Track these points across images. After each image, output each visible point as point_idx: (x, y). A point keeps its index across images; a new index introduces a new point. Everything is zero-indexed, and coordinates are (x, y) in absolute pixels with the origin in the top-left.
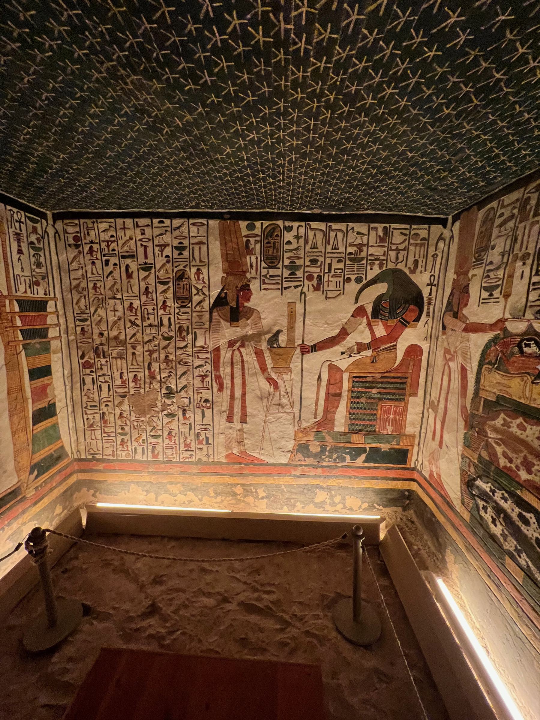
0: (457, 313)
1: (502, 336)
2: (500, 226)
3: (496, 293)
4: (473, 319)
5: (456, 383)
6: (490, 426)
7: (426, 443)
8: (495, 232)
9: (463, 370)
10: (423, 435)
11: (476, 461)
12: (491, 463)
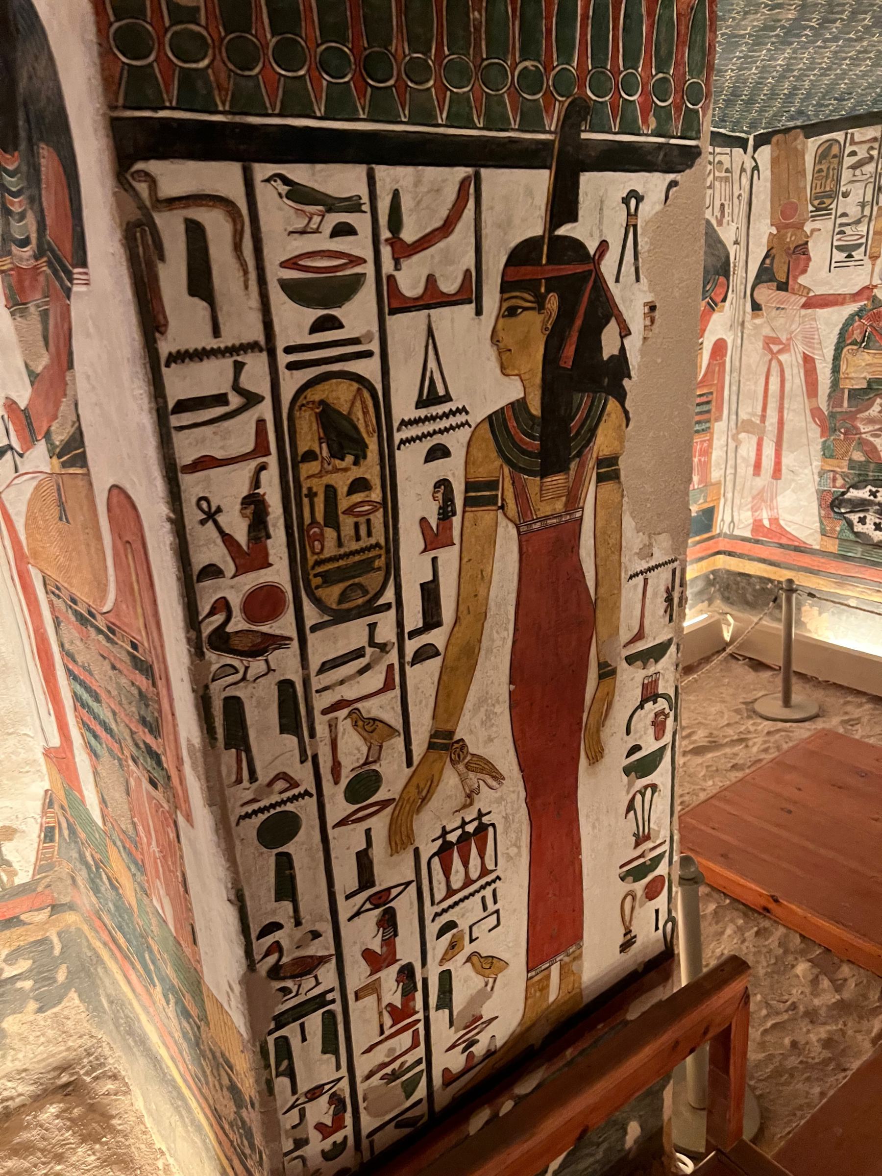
0: (787, 283)
1: (870, 307)
2: (854, 167)
3: (858, 254)
4: (819, 290)
5: (796, 379)
6: (862, 420)
7: (738, 488)
8: (846, 175)
9: (808, 361)
10: (730, 478)
11: (845, 470)
12: (868, 462)
